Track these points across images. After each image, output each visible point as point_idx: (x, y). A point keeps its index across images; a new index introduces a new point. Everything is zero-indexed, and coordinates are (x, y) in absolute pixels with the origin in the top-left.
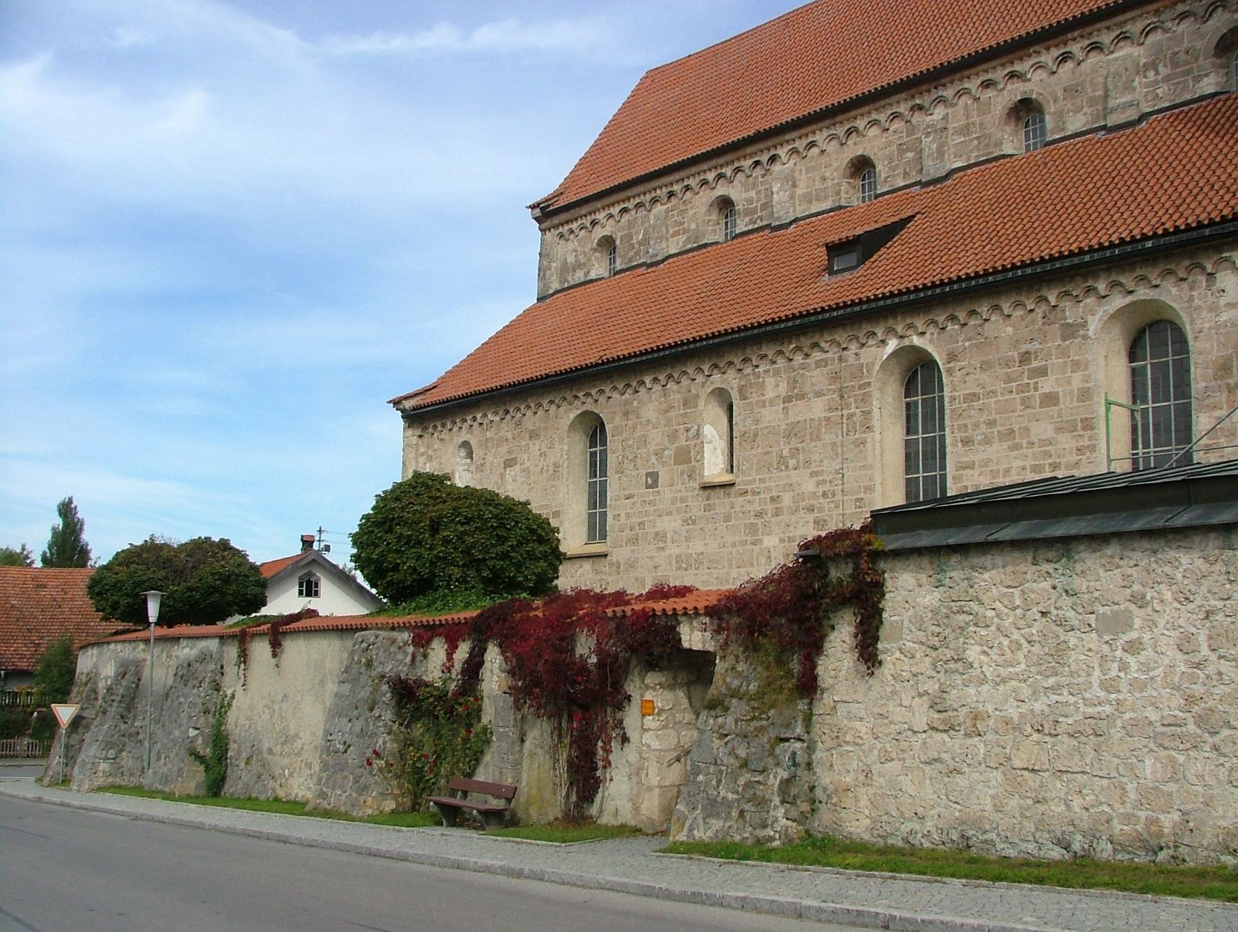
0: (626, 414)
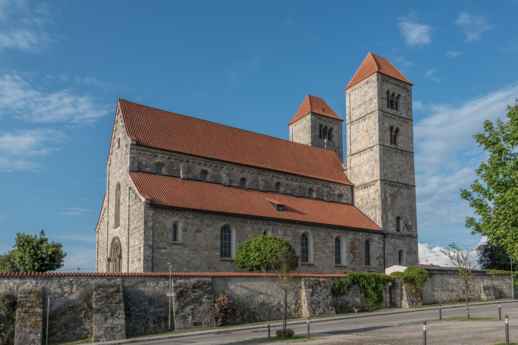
0: (241, 228)
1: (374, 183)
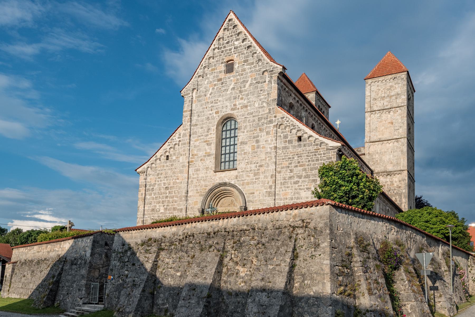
1: (399, 172)
